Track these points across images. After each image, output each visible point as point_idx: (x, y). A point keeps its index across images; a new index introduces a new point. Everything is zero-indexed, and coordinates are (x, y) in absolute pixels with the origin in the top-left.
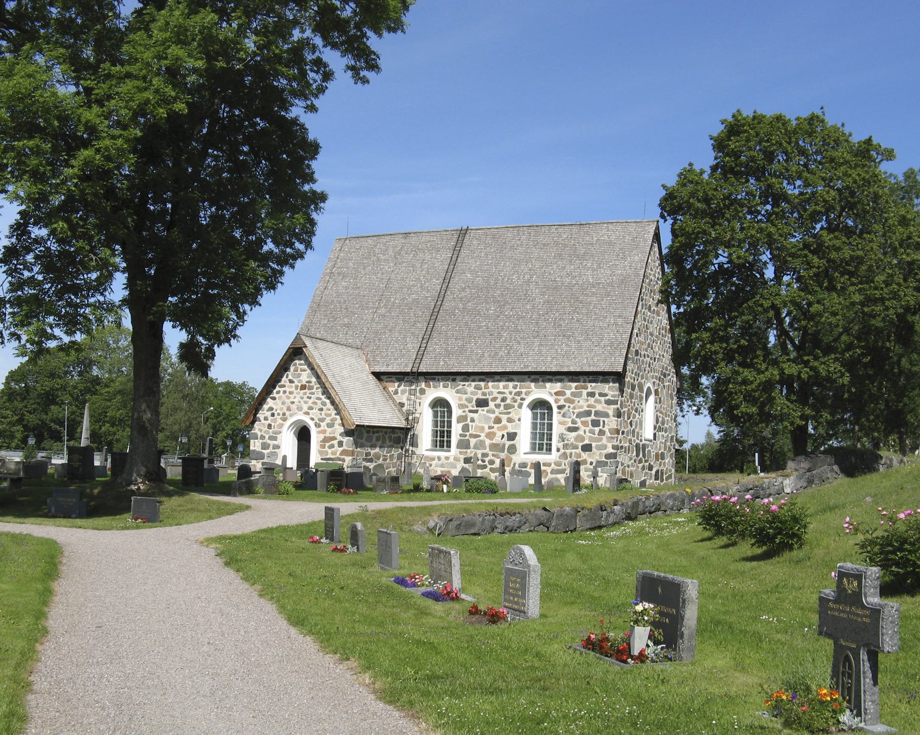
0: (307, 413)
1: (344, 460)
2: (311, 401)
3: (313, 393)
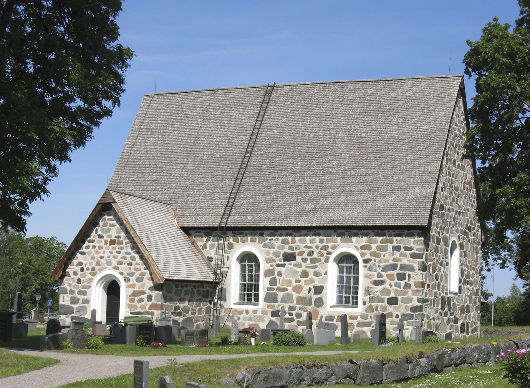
0: (116, 268)
1: (153, 314)
2: (120, 256)
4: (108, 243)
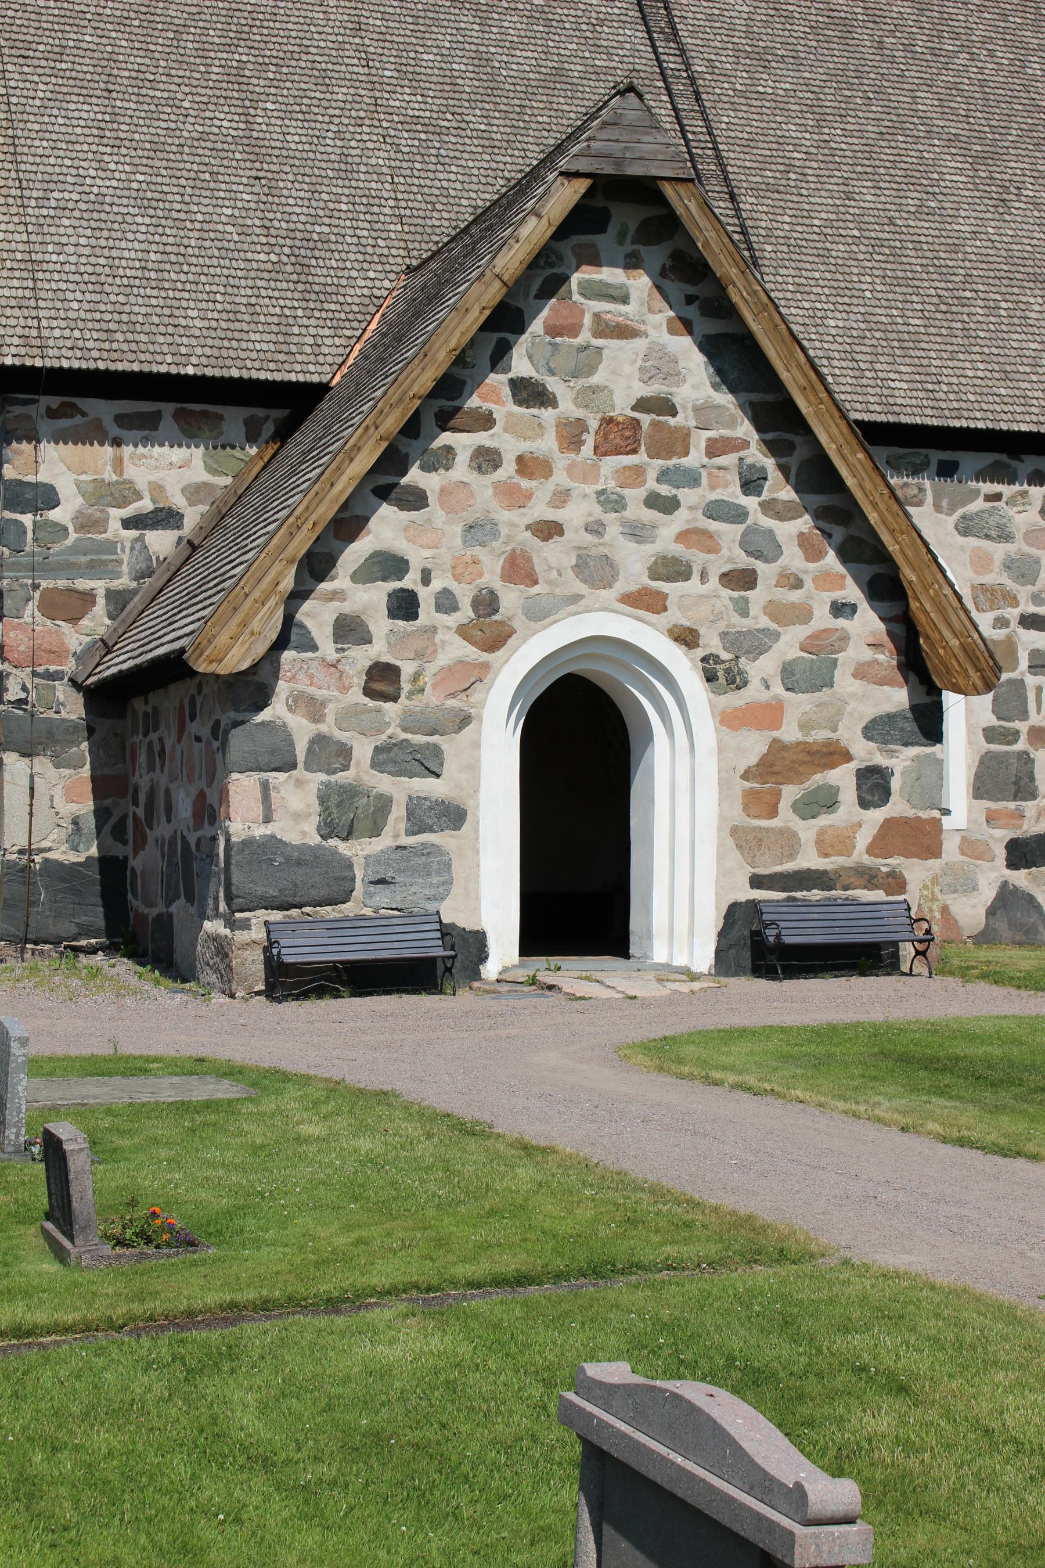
0: (647, 602)
1: (896, 882)
2: (667, 532)
3: (692, 479)
4: (590, 440)
